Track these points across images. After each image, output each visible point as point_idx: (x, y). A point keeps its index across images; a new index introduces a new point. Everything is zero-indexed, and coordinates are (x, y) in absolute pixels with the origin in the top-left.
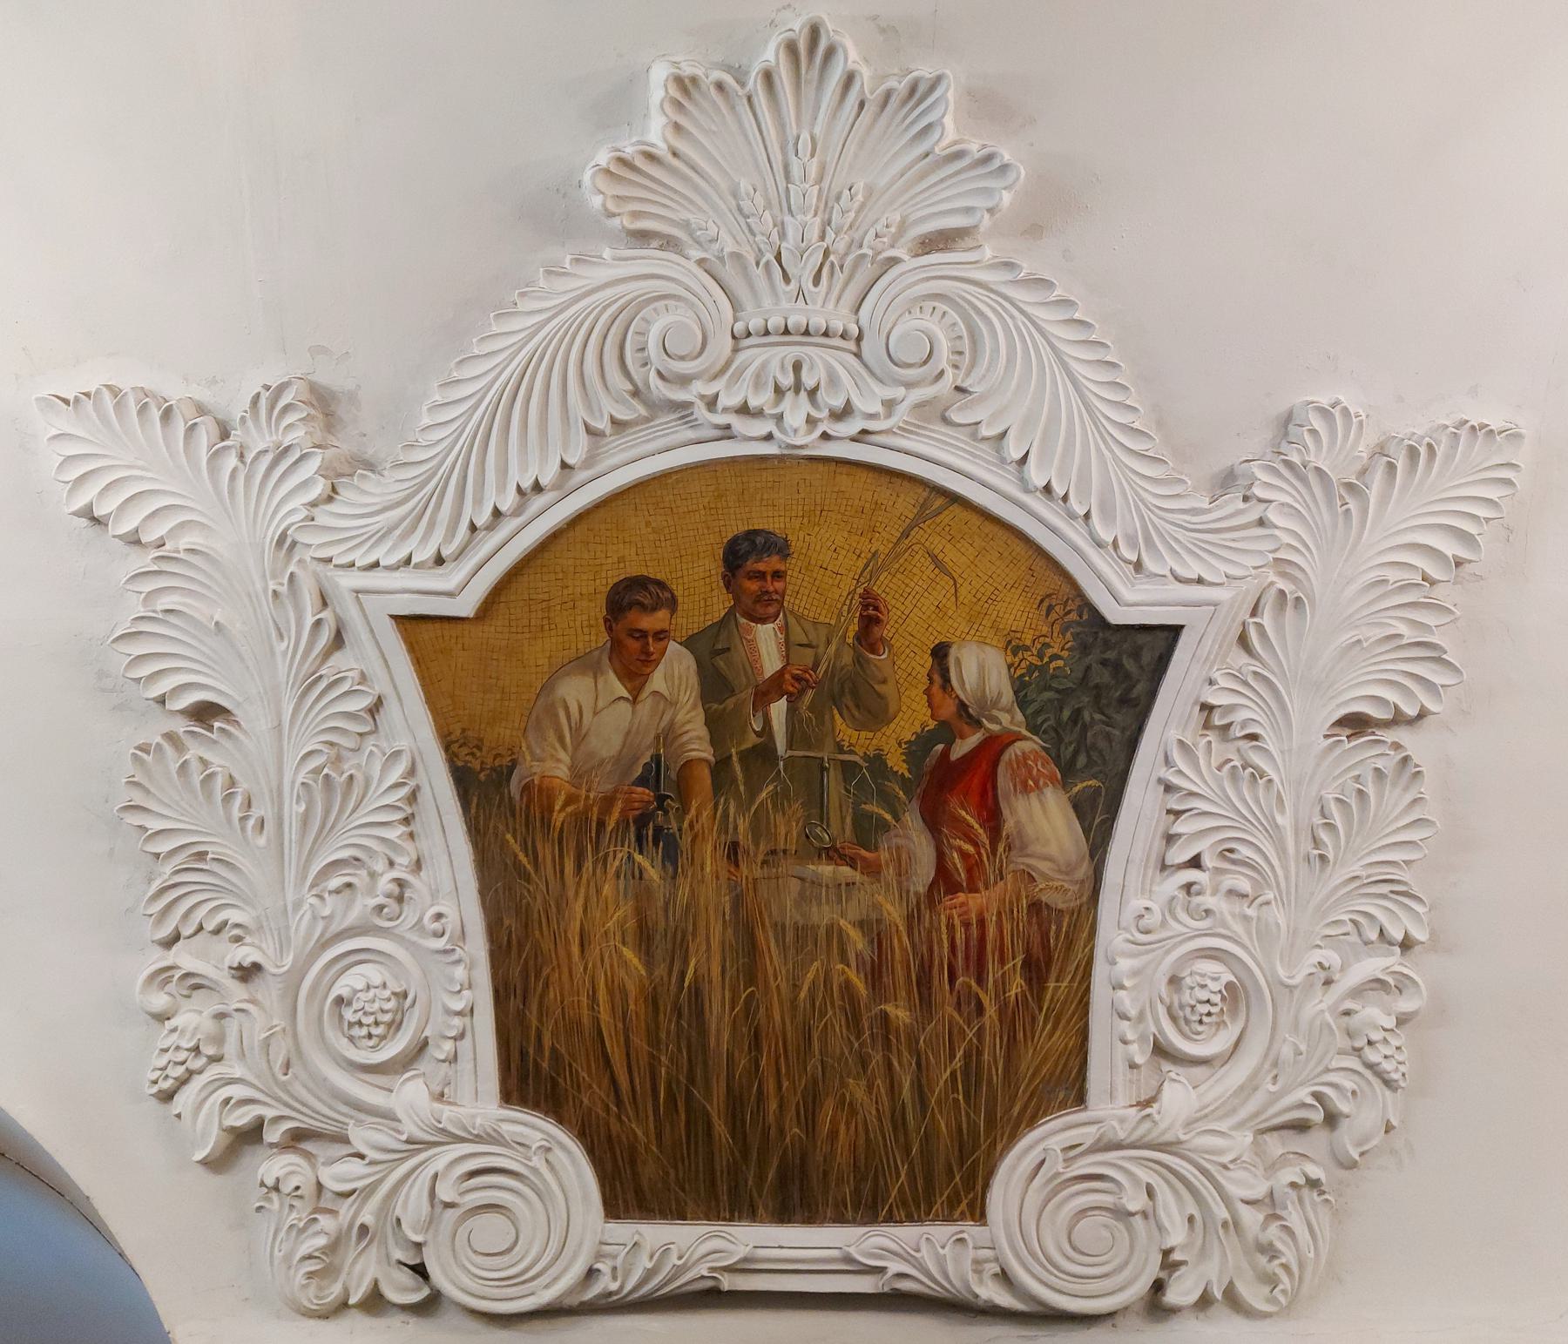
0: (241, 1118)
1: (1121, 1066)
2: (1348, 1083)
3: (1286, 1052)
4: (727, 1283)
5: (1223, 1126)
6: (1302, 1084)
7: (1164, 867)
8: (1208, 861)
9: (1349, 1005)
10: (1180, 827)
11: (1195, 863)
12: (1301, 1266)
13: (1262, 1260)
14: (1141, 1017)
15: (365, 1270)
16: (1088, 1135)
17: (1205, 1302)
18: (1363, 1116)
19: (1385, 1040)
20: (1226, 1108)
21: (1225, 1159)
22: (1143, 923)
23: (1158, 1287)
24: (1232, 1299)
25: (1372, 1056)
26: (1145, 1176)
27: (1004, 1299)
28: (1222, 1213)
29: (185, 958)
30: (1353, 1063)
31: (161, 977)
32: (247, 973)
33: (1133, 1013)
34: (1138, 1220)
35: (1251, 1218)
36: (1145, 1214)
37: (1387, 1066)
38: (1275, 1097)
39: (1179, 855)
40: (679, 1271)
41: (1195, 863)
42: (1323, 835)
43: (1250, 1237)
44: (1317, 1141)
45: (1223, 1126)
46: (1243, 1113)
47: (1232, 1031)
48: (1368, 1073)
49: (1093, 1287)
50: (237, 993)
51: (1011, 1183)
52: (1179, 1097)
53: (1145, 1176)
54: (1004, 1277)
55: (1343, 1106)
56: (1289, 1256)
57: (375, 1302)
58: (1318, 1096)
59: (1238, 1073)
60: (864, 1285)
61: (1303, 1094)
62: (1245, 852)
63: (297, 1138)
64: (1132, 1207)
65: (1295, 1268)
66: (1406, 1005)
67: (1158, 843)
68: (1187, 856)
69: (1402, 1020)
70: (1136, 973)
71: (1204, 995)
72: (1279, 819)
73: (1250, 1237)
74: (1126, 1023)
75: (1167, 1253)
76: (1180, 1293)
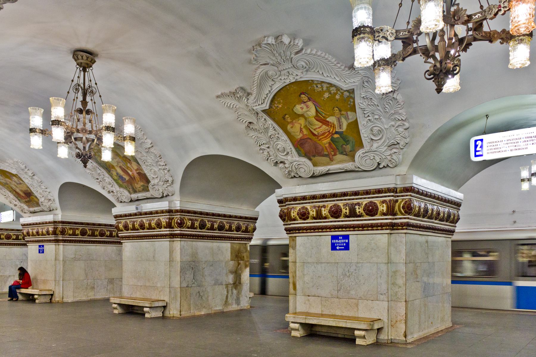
0: (275, 161)
10: (365, 112)
11: (369, 116)
15: (293, 174)
16: (364, 151)
17: (384, 167)
20: (381, 145)
27: (360, 170)
29: (262, 147)
31: (261, 149)
32: (268, 147)
41: (369, 116)
47: (381, 135)
50: (268, 150)
52: (375, 145)
57: (295, 177)
60: (343, 170)
63: (281, 162)
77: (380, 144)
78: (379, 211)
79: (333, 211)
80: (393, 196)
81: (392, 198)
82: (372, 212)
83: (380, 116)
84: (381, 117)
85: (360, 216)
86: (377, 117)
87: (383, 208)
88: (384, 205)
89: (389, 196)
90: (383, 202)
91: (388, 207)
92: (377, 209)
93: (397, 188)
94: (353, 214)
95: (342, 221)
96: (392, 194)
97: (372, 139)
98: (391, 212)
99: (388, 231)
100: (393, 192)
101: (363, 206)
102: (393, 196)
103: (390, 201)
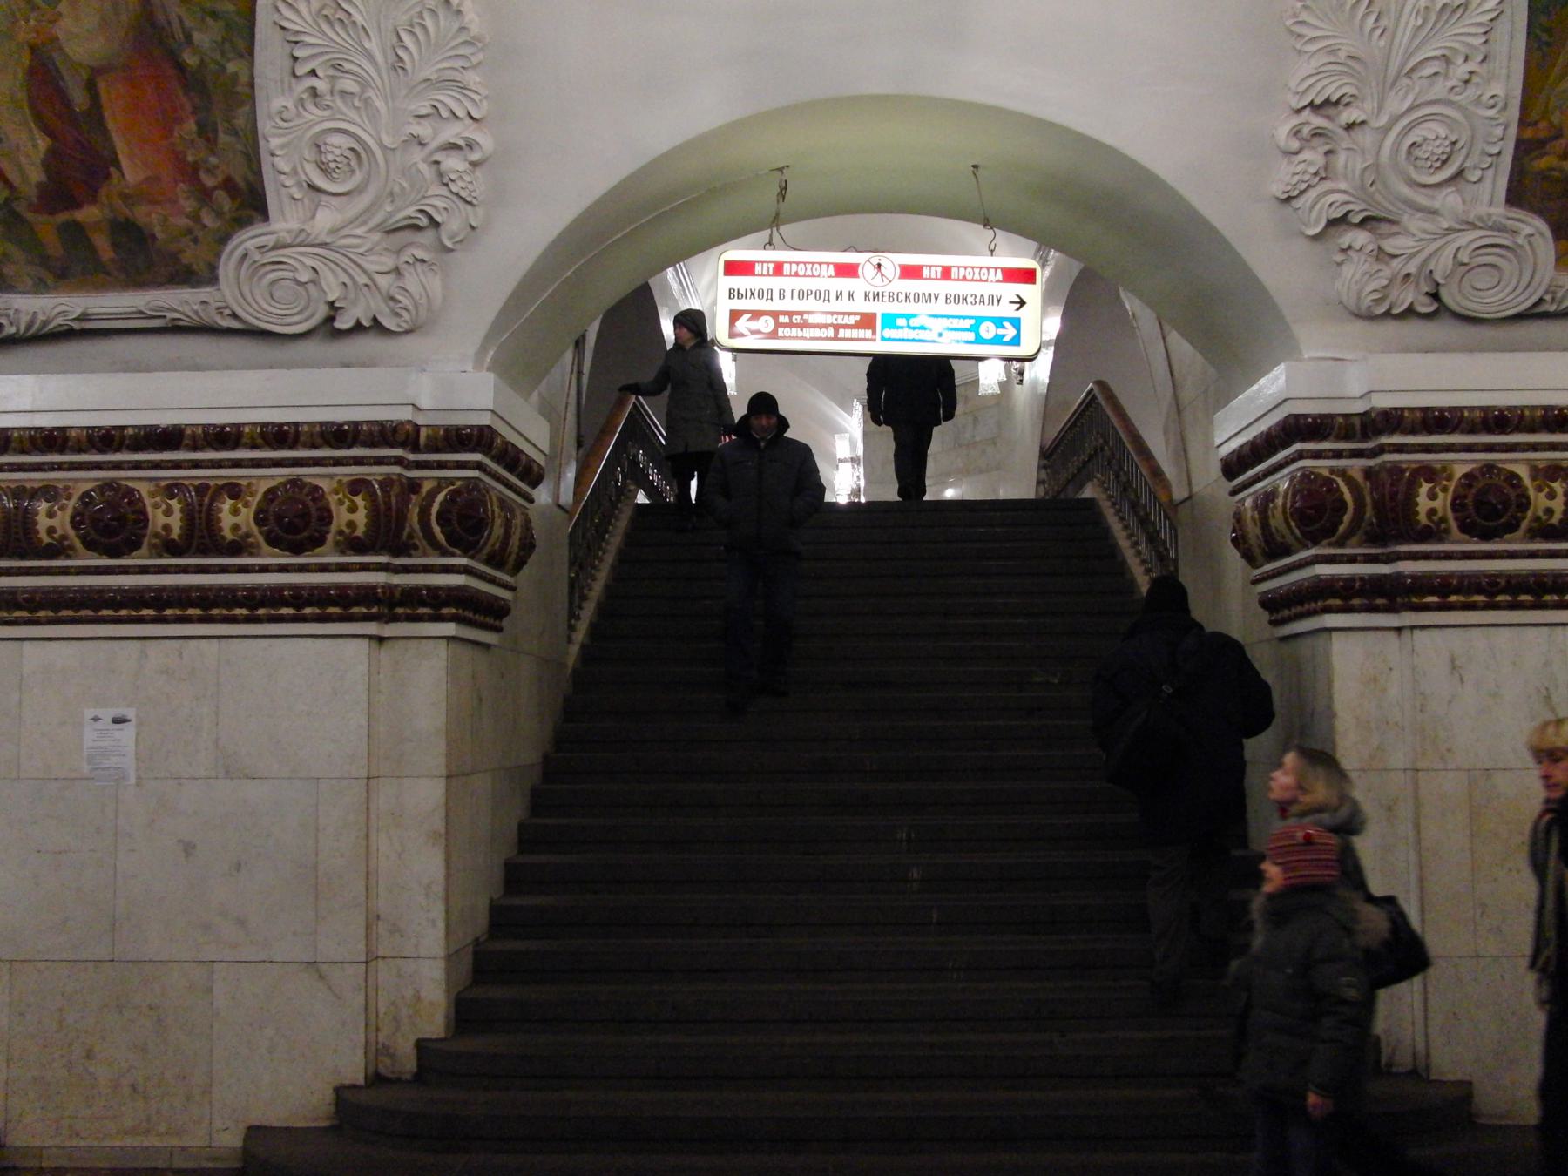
1: (286, 200)
2: (440, 203)
3: (397, 189)
4: (76, 326)
5: (359, 231)
6: (412, 204)
7: (294, 75)
8: (320, 73)
9: (437, 157)
11: (313, 73)
12: (416, 306)
13: (391, 304)
14: (295, 172)
16: (270, 240)
18: (453, 225)
19: (461, 178)
20: (360, 218)
21: (361, 250)
22: (285, 115)
23: (330, 319)
24: (377, 326)
25: (454, 188)
26: (309, 262)
28: (365, 280)
30: (444, 191)
33: (287, 169)
34: (311, 287)
35: (383, 281)
36: (313, 282)
37: (463, 194)
38: (391, 214)
39: (302, 70)
40: (45, 323)
41: (313, 73)
42: (401, 53)
43: (384, 291)
44: (427, 237)
45: (359, 231)
46: (371, 224)
47: (358, 177)
48: (454, 198)
49: (289, 320)
51: (227, 268)
52: (325, 219)
53: (309, 262)
54: (234, 316)
55: (439, 219)
56: (405, 301)
58: (422, 211)
59: (364, 201)
61: (411, 211)
62: (347, 66)
64: (303, 279)
65: (411, 307)
66: (475, 157)
67: (288, 63)
68: (308, 68)
69: (474, 164)
70: (282, 147)
71: (330, 157)
72: (367, 45)
73: (384, 291)
74: (283, 177)
75: (331, 304)
76: (343, 323)
77: (351, 212)
78: (333, 528)
79: (95, 522)
80: (399, 461)
81: (397, 469)
82: (297, 531)
83: (364, 84)
84: (371, 93)
85: (236, 548)
86: (349, 84)
87: (352, 515)
88: (359, 500)
89: (379, 461)
90: (357, 486)
91: (374, 513)
92: (326, 517)
93: (417, 428)
94: (201, 536)
95: (144, 570)
96: (398, 452)
97: (312, 187)
98: (387, 535)
99: (372, 628)
100: (403, 445)
101: (254, 501)
102: (399, 461)
103: (386, 483)
